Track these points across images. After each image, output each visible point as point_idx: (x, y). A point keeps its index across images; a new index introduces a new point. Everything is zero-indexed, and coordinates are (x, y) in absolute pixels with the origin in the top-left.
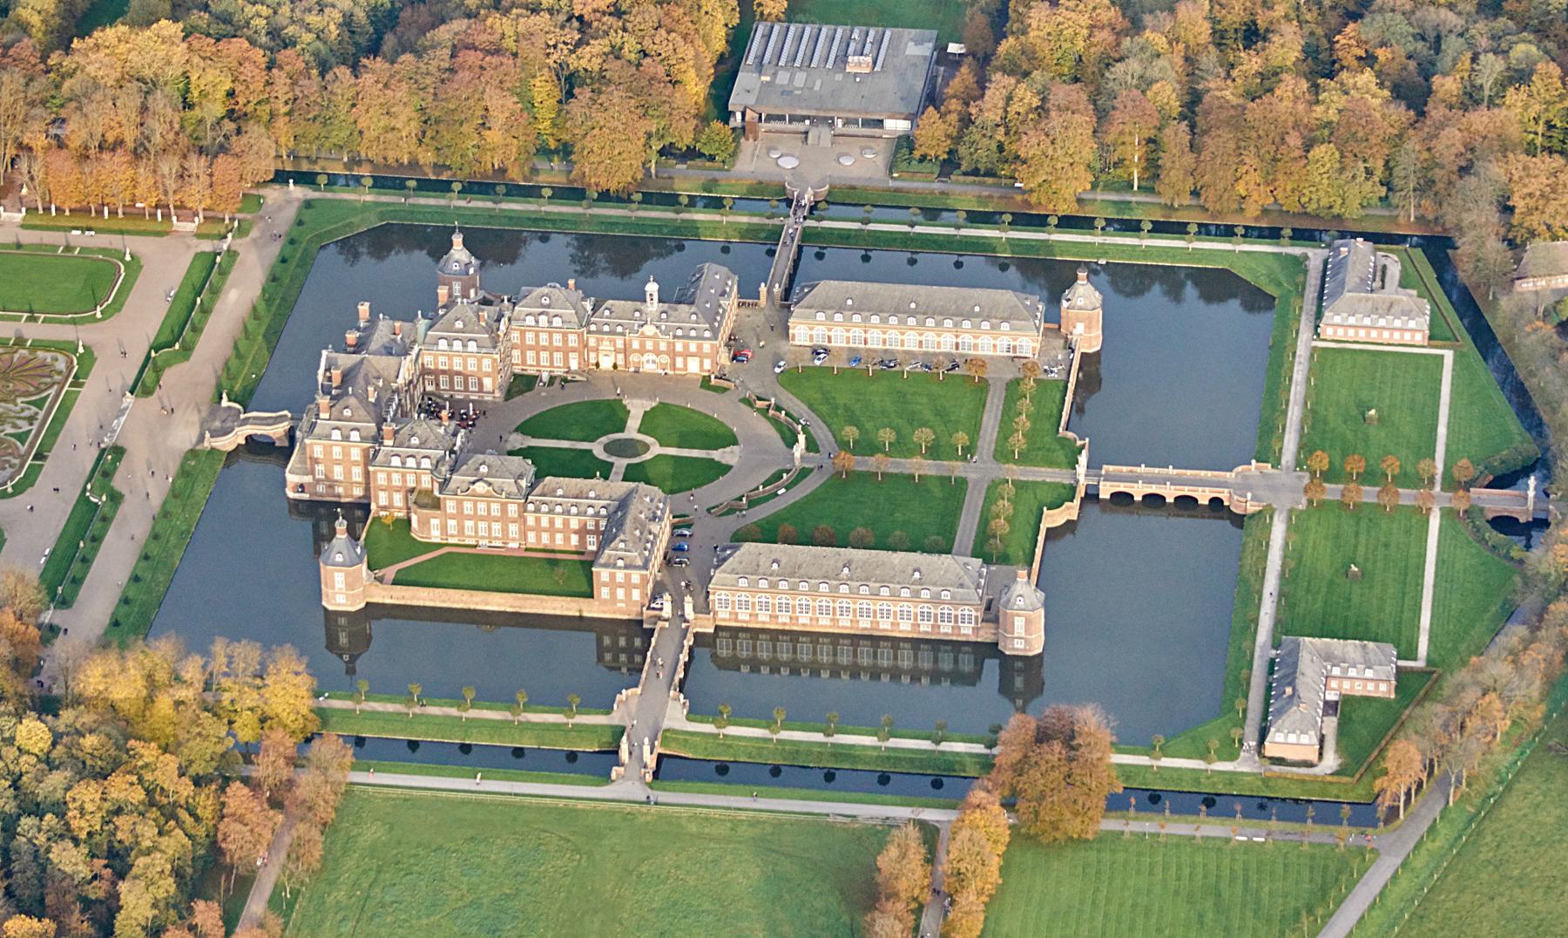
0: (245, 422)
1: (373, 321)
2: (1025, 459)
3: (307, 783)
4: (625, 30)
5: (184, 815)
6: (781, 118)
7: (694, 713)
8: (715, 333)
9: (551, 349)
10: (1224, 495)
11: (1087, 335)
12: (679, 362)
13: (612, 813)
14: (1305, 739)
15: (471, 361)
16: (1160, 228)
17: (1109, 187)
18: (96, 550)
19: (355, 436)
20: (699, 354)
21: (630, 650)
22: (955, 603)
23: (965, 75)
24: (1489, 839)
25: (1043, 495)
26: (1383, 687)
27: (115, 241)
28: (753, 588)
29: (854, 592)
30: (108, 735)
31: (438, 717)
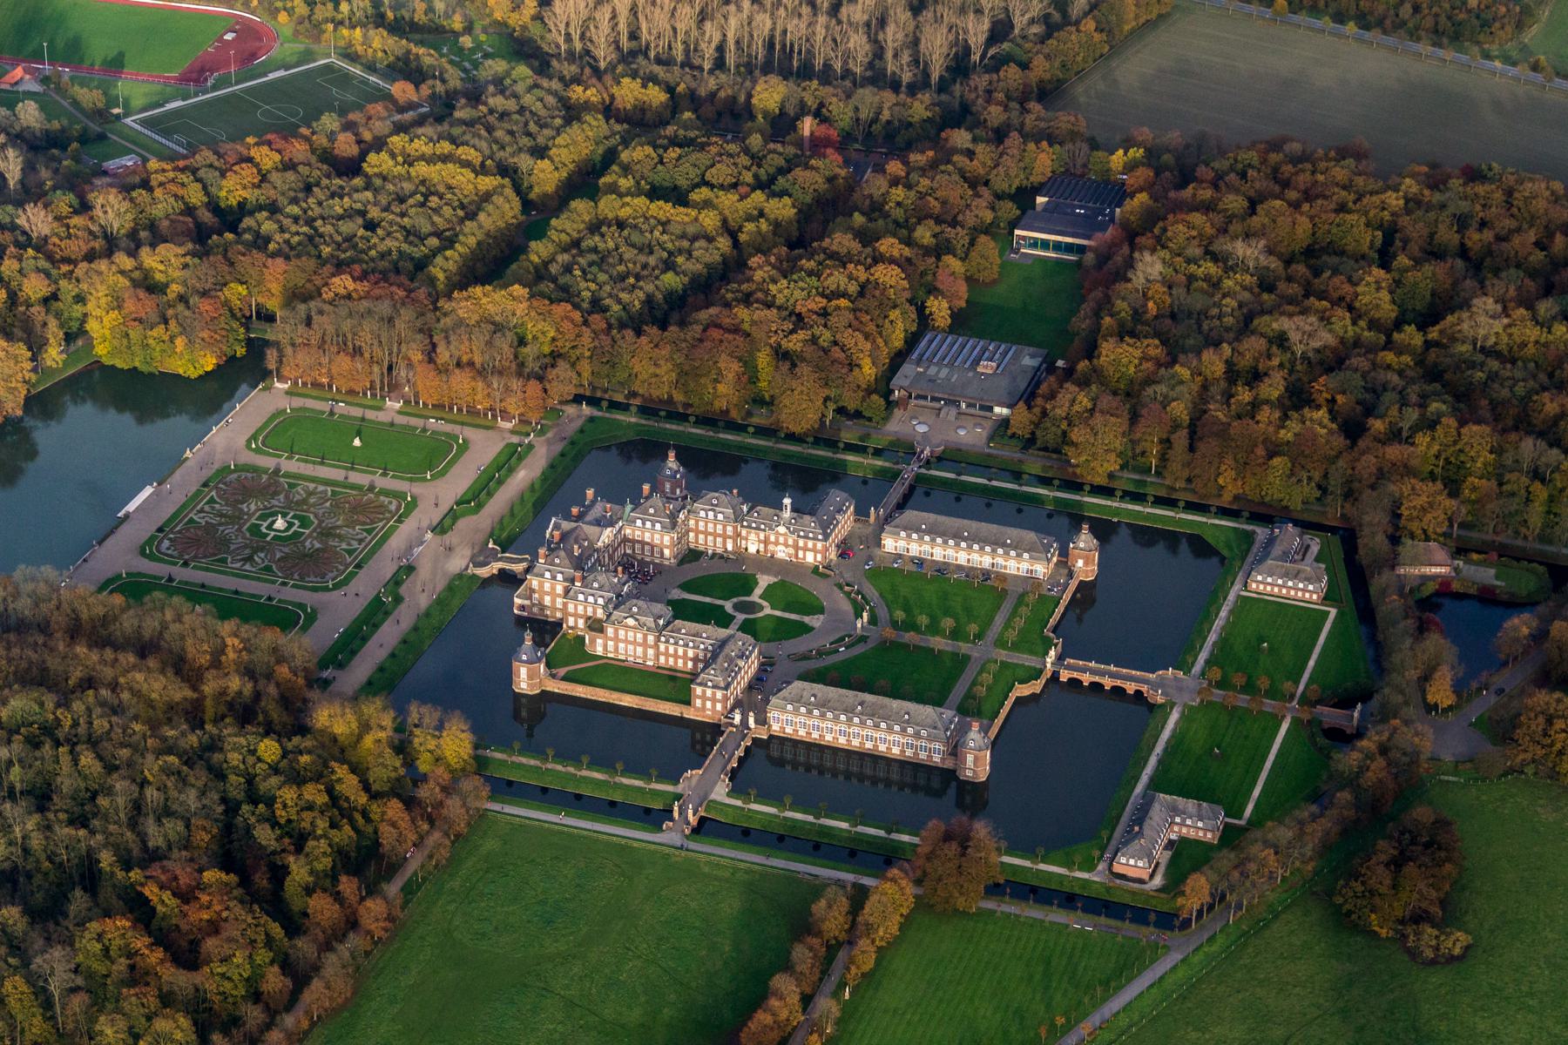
0: (500, 559)
1: (594, 502)
2: (1015, 647)
3: (453, 807)
4: (825, 326)
5: (358, 817)
6: (925, 398)
7: (734, 791)
8: (826, 538)
9: (715, 535)
10: (1144, 688)
11: (1085, 566)
12: (801, 554)
13: (654, 852)
14: (1140, 864)
15: (657, 536)
16: (1160, 501)
17: (1136, 470)
18: (373, 633)
19: (560, 577)
20: (814, 550)
22: (930, 739)
24: (1250, 950)
25: (1021, 673)
26: (1209, 835)
27: (457, 429)
28: (796, 712)
29: (863, 723)
30: (319, 756)
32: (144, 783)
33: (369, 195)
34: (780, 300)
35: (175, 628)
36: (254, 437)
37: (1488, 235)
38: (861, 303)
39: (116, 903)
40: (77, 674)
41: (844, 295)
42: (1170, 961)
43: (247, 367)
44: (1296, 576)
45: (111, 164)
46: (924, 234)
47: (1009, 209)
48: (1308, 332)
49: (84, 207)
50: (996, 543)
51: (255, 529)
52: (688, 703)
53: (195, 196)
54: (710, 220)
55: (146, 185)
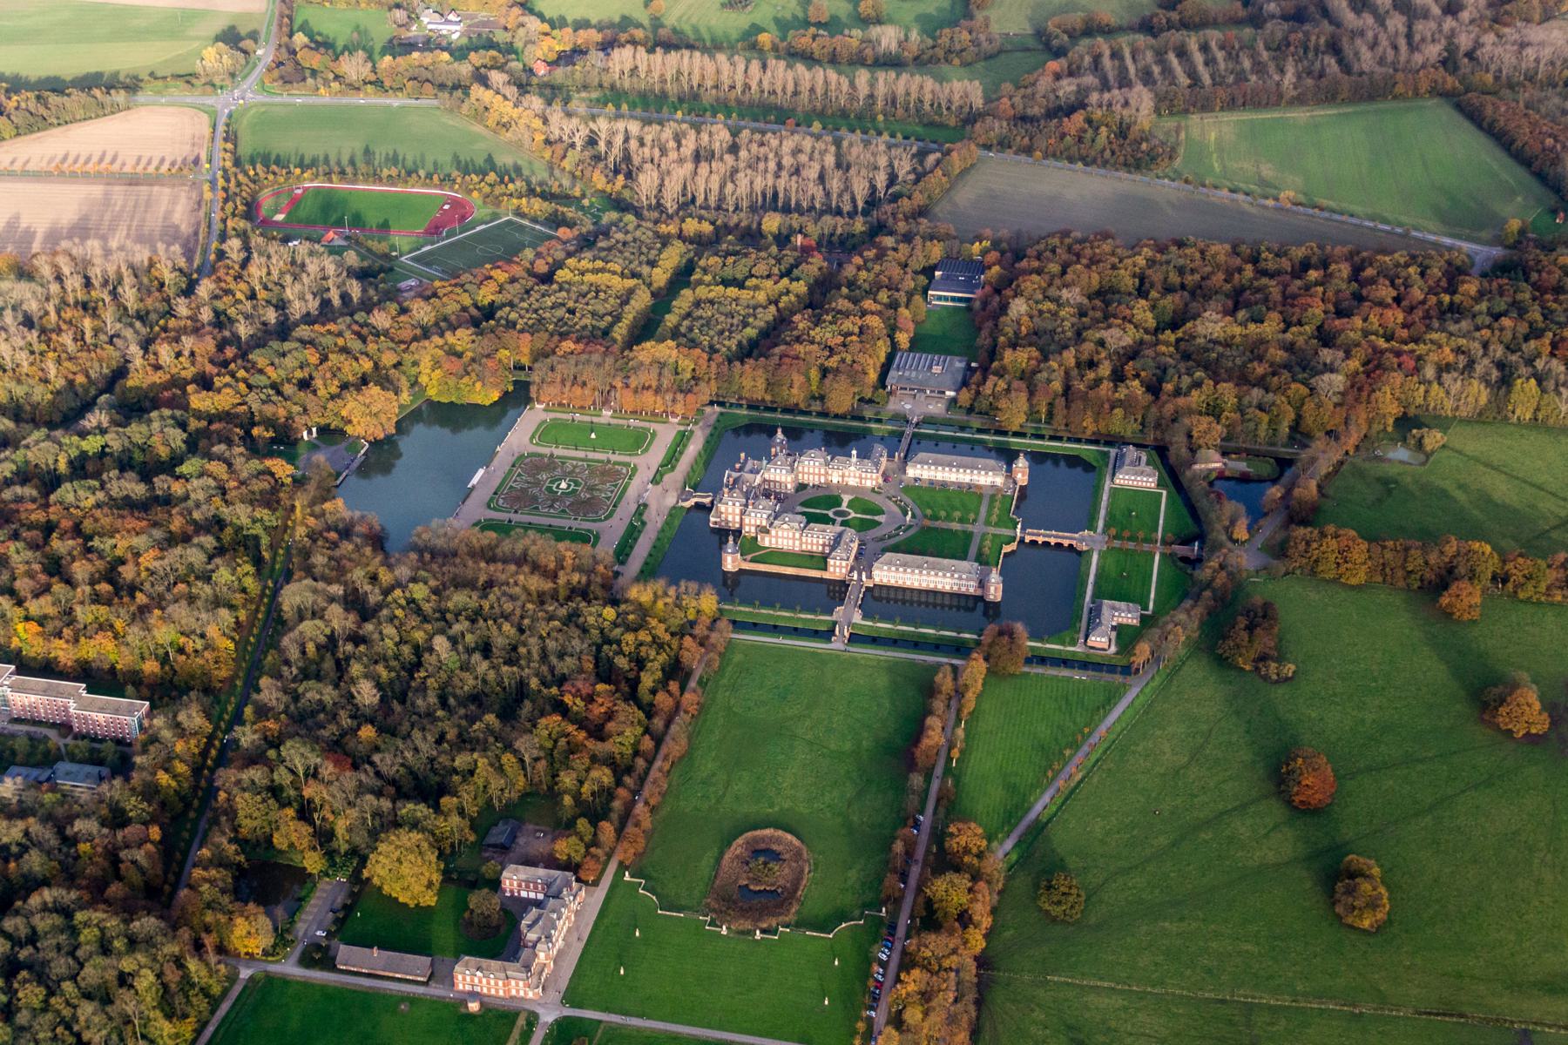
1: (746, 460)
2: (996, 525)
3: (714, 637)
7: (865, 617)
16: (1052, 438)
21: (840, 592)
23: (977, 376)
27: (646, 425)
31: (765, 614)
32: (541, 637)
33: (564, 294)
34: (818, 339)
35: (533, 548)
36: (533, 437)
37: (1197, 277)
38: (864, 337)
39: (548, 708)
40: (482, 579)
41: (851, 334)
42: (1134, 694)
43: (519, 396)
44: (1142, 473)
45: (403, 285)
46: (883, 296)
47: (923, 280)
48: (1119, 337)
49: (404, 311)
50: (973, 467)
51: (549, 489)
52: (825, 569)
53: (467, 302)
54: (761, 297)
55: (435, 295)
